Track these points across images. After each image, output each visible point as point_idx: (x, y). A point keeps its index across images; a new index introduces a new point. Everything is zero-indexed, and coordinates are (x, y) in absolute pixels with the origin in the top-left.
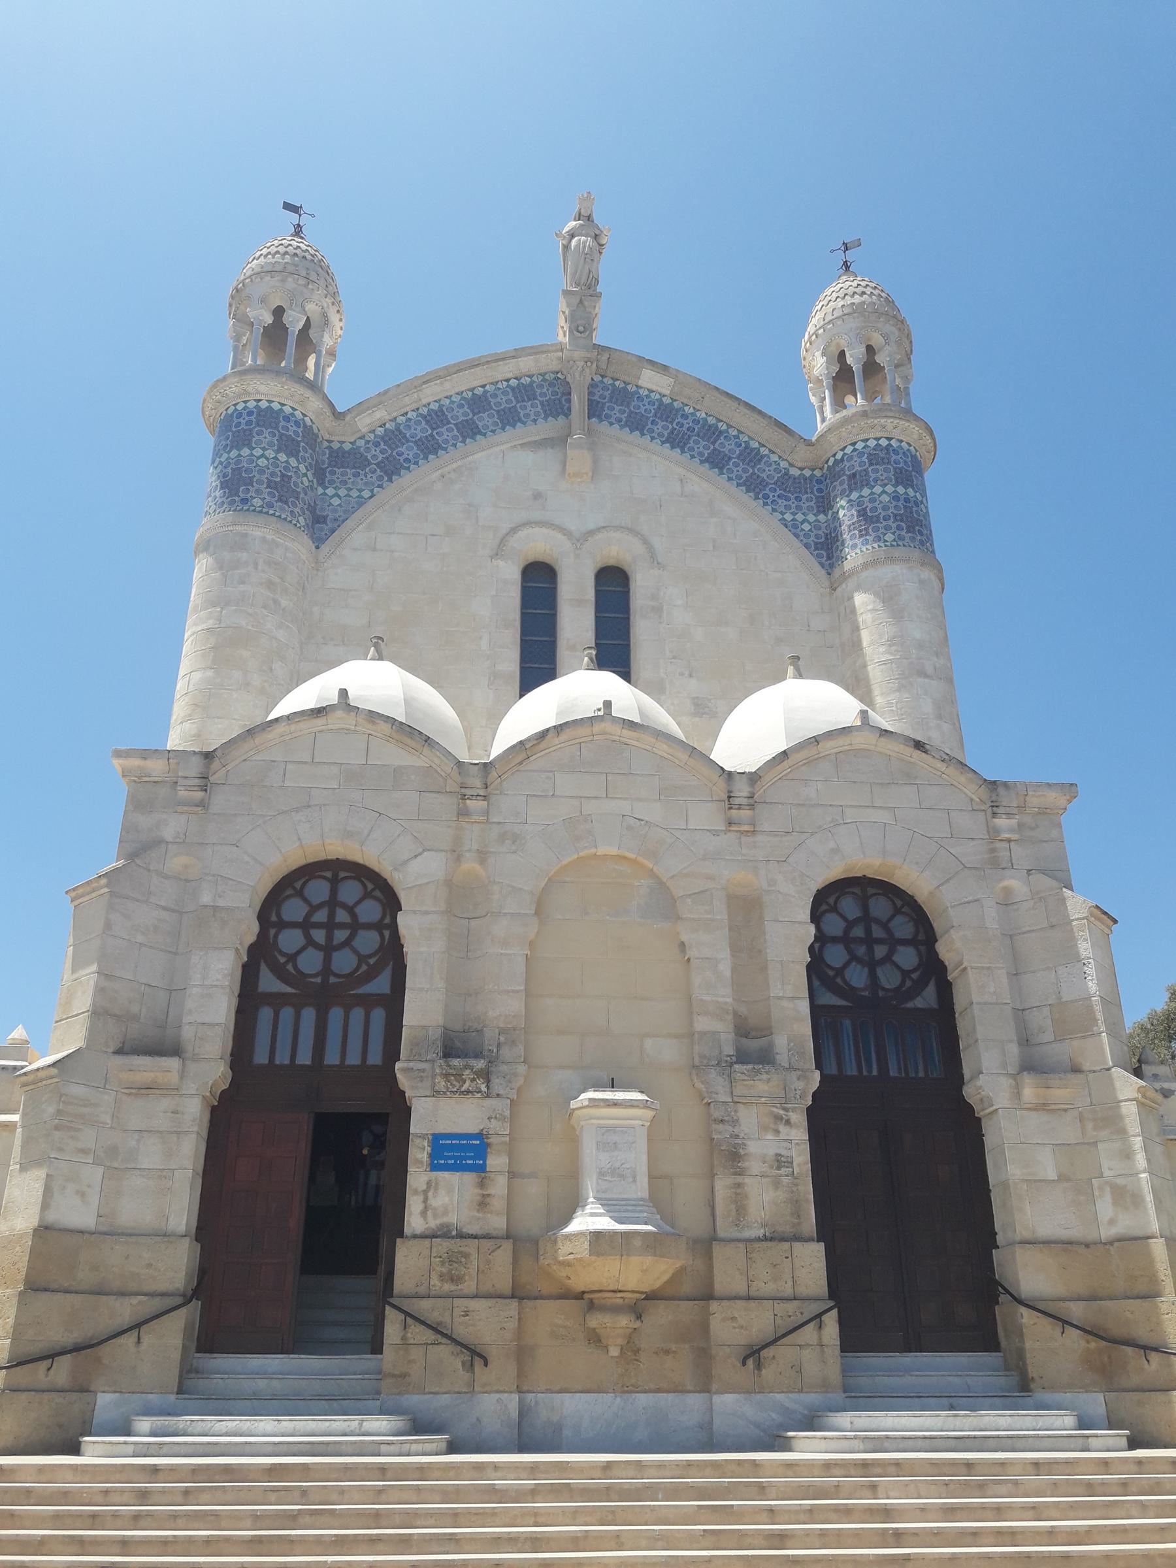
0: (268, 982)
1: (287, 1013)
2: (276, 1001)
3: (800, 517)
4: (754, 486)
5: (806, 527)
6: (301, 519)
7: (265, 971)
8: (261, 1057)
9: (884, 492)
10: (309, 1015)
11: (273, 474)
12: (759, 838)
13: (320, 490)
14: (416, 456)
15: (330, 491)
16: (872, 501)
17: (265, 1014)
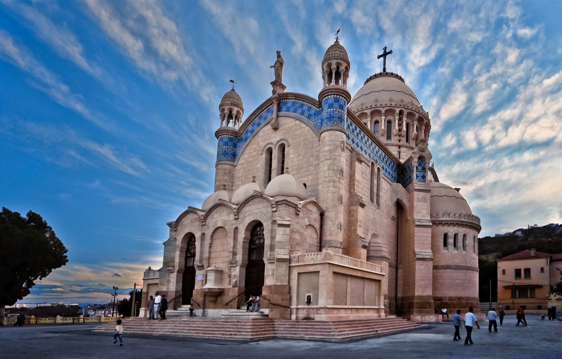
0: (189, 255)
1: (190, 258)
2: (189, 257)
3: (318, 122)
4: (309, 117)
5: (319, 124)
6: (229, 158)
7: (188, 253)
8: (188, 265)
9: (325, 112)
10: (192, 259)
11: (223, 151)
12: (239, 220)
13: (236, 149)
14: (250, 135)
15: (237, 149)
16: (333, 112)
17: (188, 259)
